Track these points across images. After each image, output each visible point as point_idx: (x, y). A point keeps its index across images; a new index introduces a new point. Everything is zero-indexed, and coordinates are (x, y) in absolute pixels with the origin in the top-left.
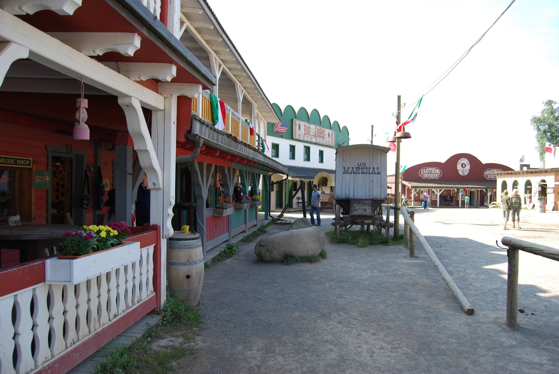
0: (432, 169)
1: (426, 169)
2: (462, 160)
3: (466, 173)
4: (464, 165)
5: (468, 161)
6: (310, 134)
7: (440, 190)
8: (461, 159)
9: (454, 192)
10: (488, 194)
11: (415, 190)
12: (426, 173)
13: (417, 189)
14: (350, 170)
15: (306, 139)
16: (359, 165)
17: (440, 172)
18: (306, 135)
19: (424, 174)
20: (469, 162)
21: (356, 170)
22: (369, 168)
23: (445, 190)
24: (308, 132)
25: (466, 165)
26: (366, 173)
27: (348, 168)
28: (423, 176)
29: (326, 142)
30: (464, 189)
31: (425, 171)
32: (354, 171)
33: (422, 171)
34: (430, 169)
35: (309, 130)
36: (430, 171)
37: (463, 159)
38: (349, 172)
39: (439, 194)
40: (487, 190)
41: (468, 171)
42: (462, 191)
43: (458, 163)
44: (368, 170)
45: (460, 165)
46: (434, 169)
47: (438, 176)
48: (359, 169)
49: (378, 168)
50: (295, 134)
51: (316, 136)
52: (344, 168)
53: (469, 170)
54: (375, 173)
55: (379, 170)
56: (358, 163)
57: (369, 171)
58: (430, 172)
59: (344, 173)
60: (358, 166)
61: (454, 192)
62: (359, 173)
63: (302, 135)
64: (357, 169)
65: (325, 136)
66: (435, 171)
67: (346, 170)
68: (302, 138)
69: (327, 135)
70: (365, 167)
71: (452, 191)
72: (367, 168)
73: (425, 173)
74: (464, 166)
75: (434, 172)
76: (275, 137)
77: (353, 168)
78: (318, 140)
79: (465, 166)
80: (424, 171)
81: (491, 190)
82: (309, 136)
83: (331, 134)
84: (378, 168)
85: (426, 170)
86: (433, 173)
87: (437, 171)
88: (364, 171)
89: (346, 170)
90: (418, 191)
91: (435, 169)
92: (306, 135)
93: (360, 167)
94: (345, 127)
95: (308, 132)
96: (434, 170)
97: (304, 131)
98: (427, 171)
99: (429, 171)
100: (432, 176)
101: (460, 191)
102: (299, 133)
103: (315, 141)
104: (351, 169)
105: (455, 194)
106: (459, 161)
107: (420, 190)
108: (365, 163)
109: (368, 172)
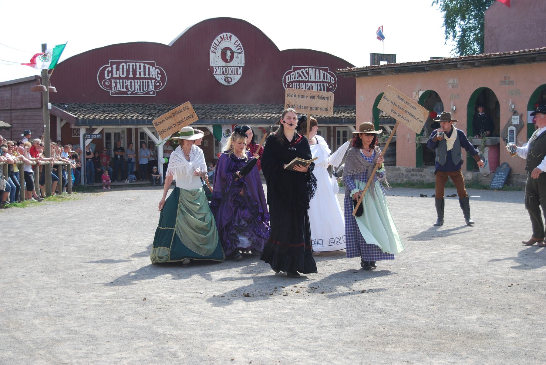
0: (138, 64)
1: (118, 64)
2: (223, 39)
3: (236, 79)
4: (229, 53)
5: (239, 42)
8: (221, 35)
11: (90, 132)
12: (120, 78)
13: (95, 129)
17: (162, 73)
19: (113, 80)
20: (241, 45)
25: (235, 55)
28: (110, 87)
31: (114, 70)
33: (106, 72)
34: (131, 64)
36: (131, 70)
37: (225, 34)
41: (240, 72)
43: (212, 49)
46: (142, 65)
47: (156, 87)
53: (244, 69)
66: (147, 73)
74: (228, 57)
75: (142, 76)
79: (232, 57)
80: (112, 72)
85: (118, 69)
86: (140, 78)
87: (151, 70)
90: (99, 136)
91: (147, 66)
96: (142, 68)
98: (121, 70)
99: (128, 70)
100: (137, 88)
106: (215, 41)
107: (101, 132)
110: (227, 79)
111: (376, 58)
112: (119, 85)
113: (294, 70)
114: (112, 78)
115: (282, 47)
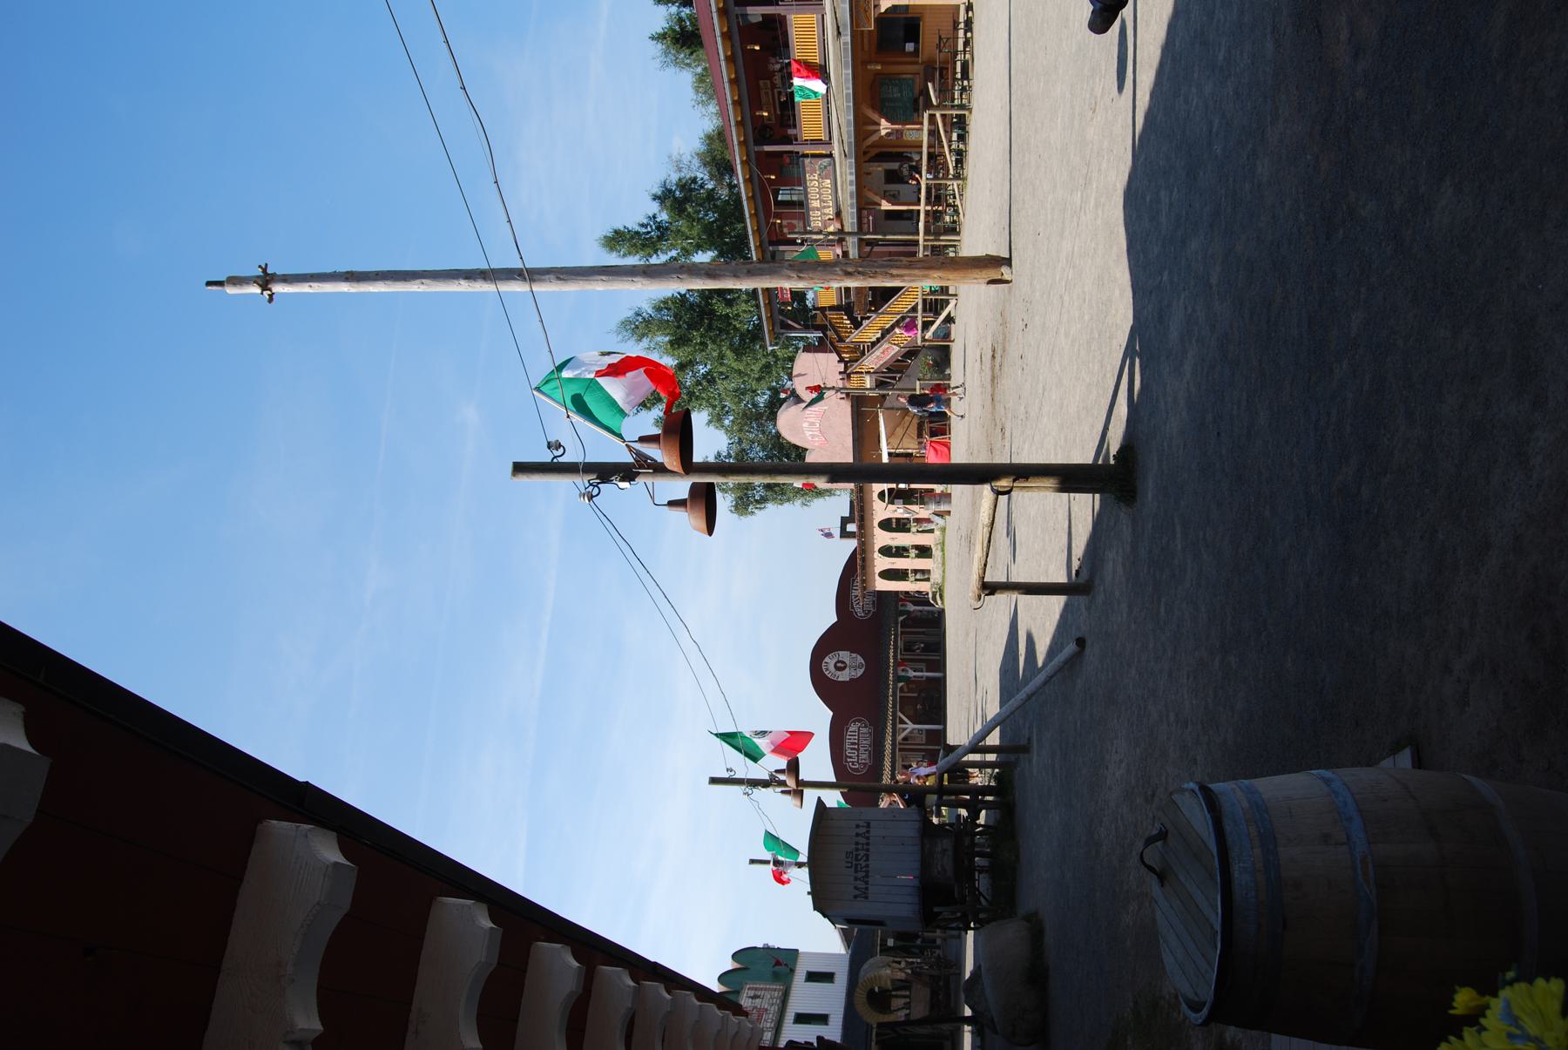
2: (827, 669)
3: (860, 660)
4: (839, 665)
7: (902, 722)
9: (906, 690)
10: (912, 610)
12: (858, 756)
14: (861, 885)
16: (850, 865)
17: (855, 721)
22: (857, 843)
23: (900, 711)
25: (840, 659)
26: (868, 850)
27: (856, 888)
30: (897, 664)
38: (864, 886)
39: (910, 726)
40: (901, 611)
41: (854, 655)
42: (903, 670)
44: (860, 847)
45: (839, 673)
47: (866, 727)
48: (859, 866)
49: (858, 826)
52: (856, 897)
54: (868, 832)
55: (861, 823)
58: (856, 747)
59: (866, 898)
60: (851, 867)
61: (906, 690)
62: (867, 866)
64: (859, 869)
67: (860, 893)
71: (903, 695)
72: (857, 850)
73: (858, 758)
77: (856, 879)
78: (768, 1025)
79: (843, 662)
80: (853, 762)
81: (900, 603)
83: (753, 992)
84: (858, 826)
85: (851, 757)
86: (859, 740)
88: (862, 855)
89: (860, 893)
91: (849, 733)
94: (735, 956)
99: (852, 749)
100: (866, 742)
101: (903, 674)
104: (859, 882)
105: (911, 686)
106: (829, 676)
109: (865, 847)
110: (860, 666)
111: (844, 534)
112: (864, 756)
113: (853, 608)
114: (858, 762)
115: (836, 620)
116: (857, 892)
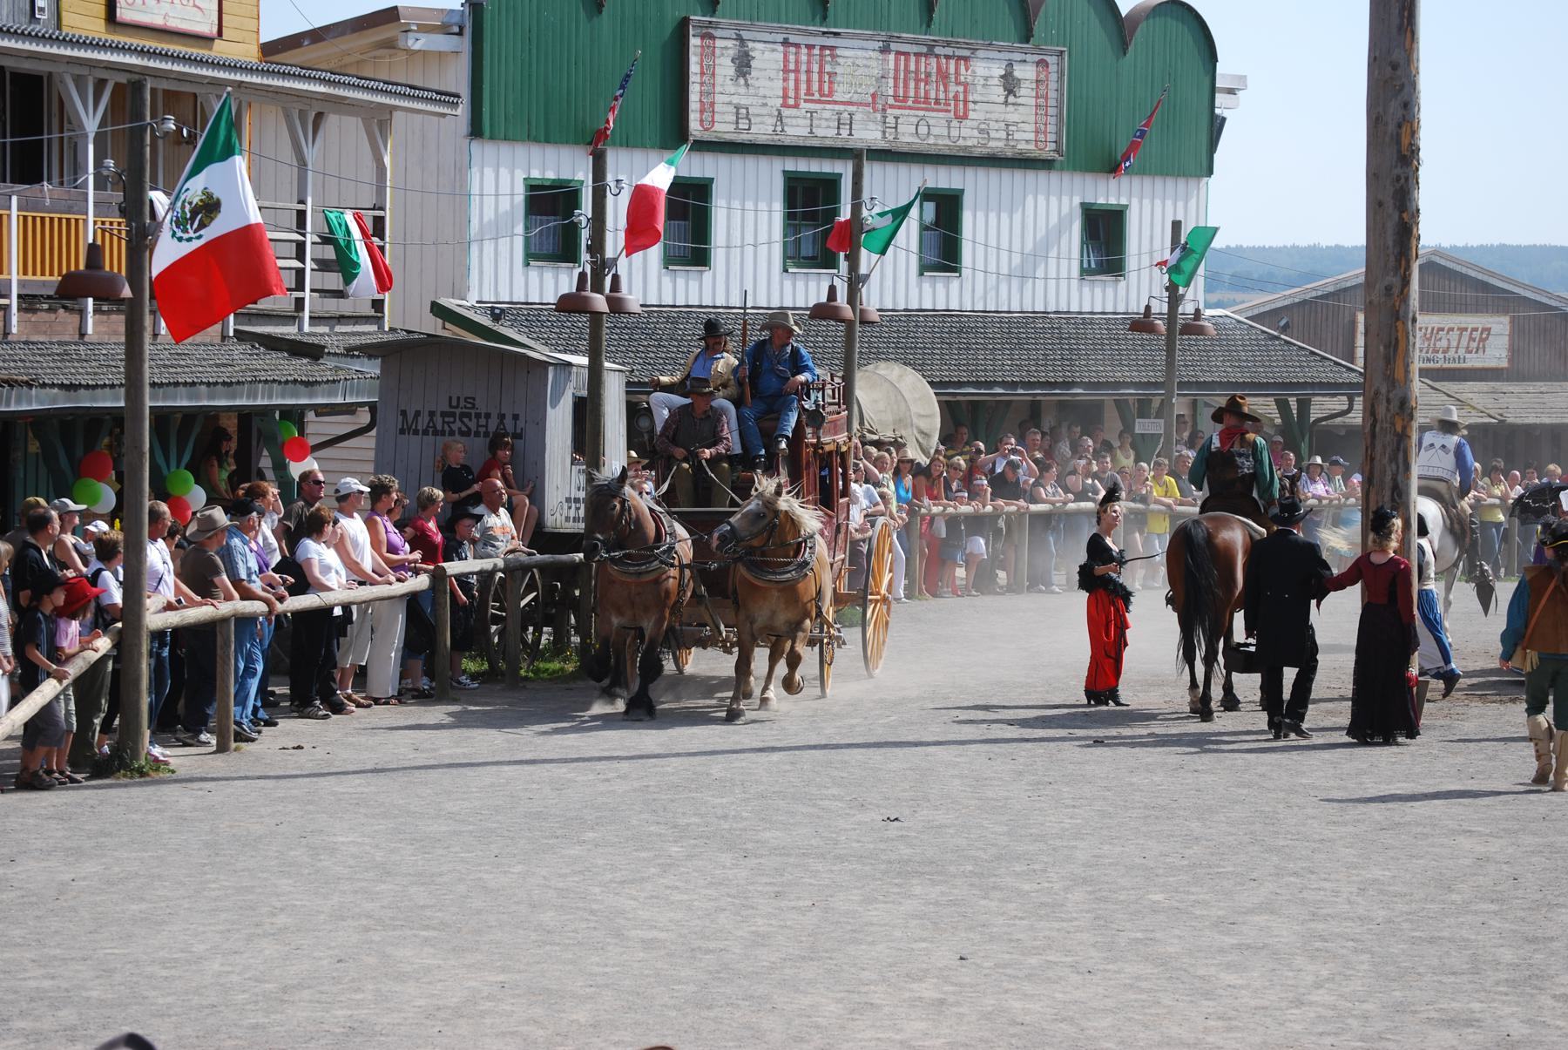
6: (835, 98)
14: (423, 422)
15: (796, 131)
16: (454, 403)
18: (796, 106)
21: (444, 422)
22: (488, 416)
24: (815, 87)
26: (477, 434)
29: (981, 131)
32: (434, 427)
35: (828, 68)
44: (483, 421)
48: (452, 419)
49: (516, 417)
50: (708, 108)
51: (891, 101)
52: (404, 413)
55: (521, 424)
56: (450, 398)
57: (486, 426)
59: (402, 432)
63: (764, 111)
64: (447, 419)
65: (970, 98)
68: (762, 131)
69: (996, 81)
70: (473, 411)
72: (478, 416)
76: (547, 141)
82: (827, 112)
84: (516, 417)
89: (410, 422)
92: (796, 106)
93: (458, 411)
95: (815, 87)
97: (780, 84)
102: (735, 100)
103: (879, 135)
104: (427, 419)
108: (474, 399)
109: (482, 430)
116: (410, 417)
